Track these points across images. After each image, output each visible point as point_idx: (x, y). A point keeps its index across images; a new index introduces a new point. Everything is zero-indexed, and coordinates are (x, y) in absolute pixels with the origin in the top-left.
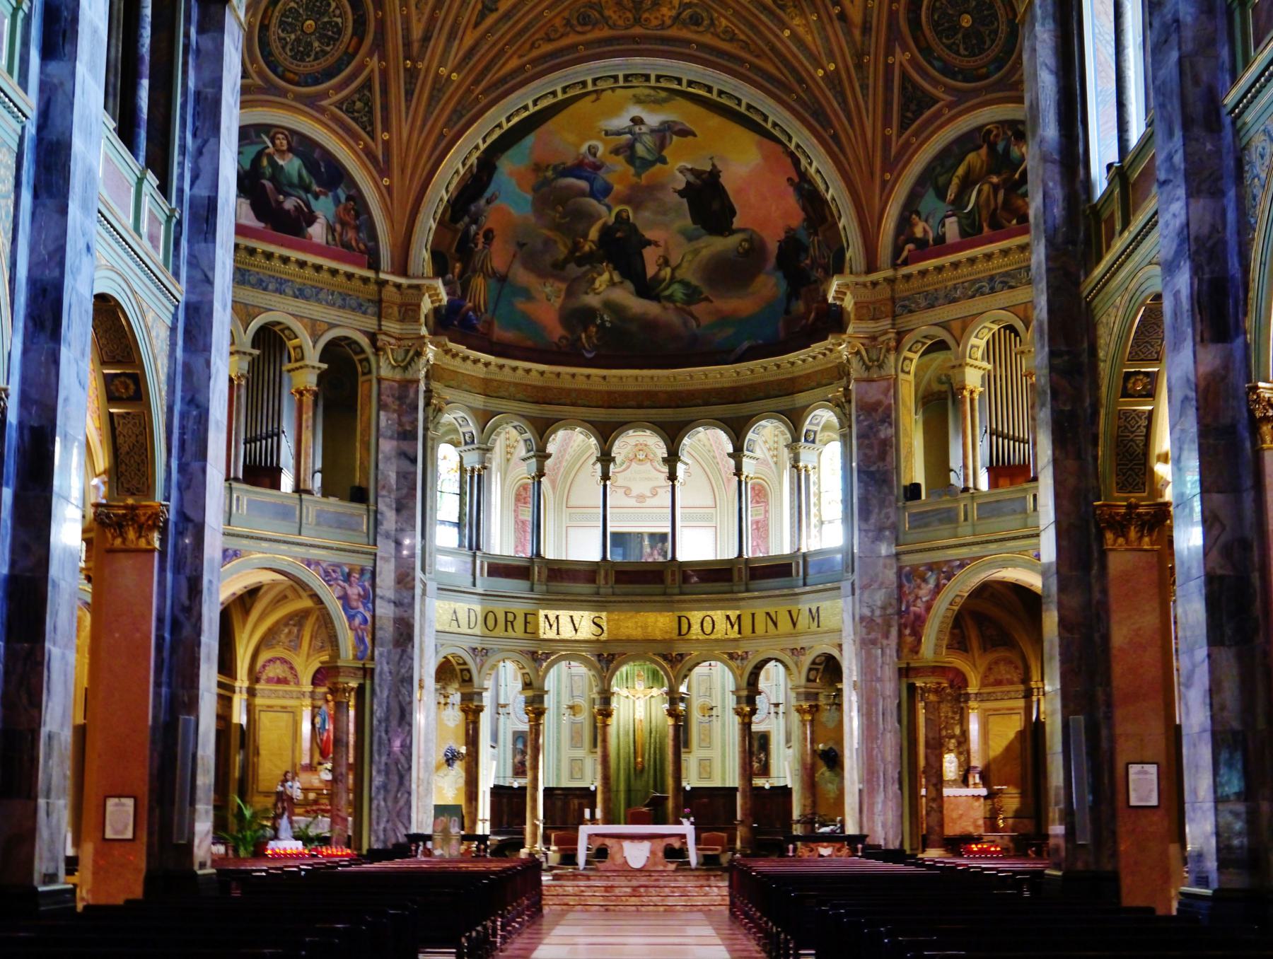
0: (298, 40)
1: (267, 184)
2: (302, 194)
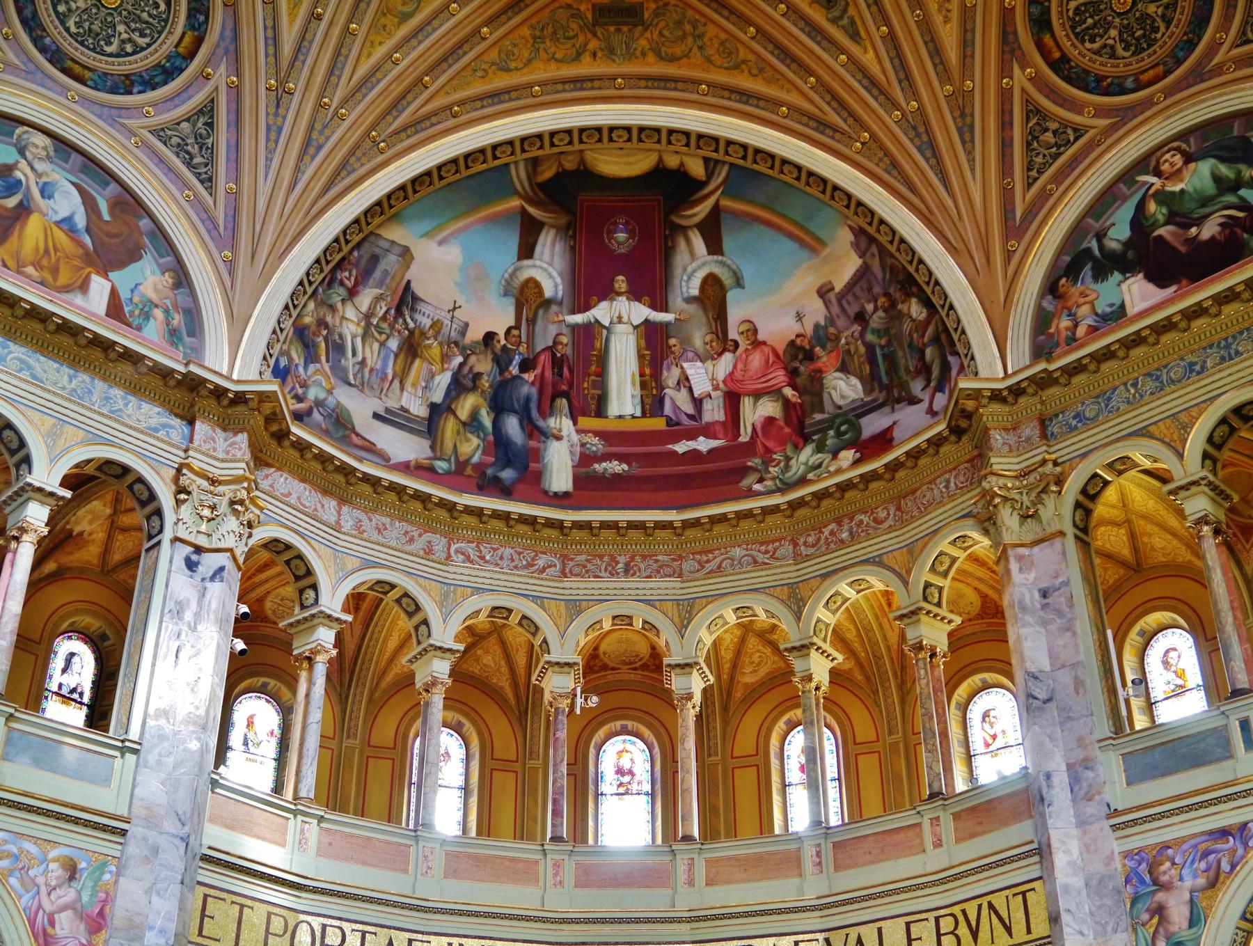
0: (1124, 29)
1: (1161, 231)
2: (1231, 198)
